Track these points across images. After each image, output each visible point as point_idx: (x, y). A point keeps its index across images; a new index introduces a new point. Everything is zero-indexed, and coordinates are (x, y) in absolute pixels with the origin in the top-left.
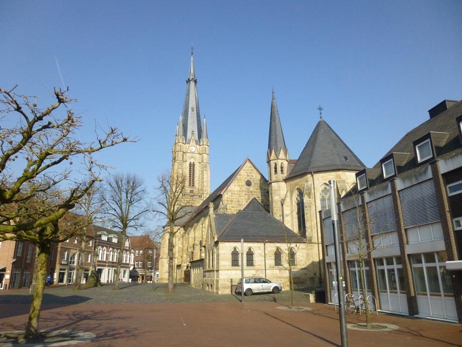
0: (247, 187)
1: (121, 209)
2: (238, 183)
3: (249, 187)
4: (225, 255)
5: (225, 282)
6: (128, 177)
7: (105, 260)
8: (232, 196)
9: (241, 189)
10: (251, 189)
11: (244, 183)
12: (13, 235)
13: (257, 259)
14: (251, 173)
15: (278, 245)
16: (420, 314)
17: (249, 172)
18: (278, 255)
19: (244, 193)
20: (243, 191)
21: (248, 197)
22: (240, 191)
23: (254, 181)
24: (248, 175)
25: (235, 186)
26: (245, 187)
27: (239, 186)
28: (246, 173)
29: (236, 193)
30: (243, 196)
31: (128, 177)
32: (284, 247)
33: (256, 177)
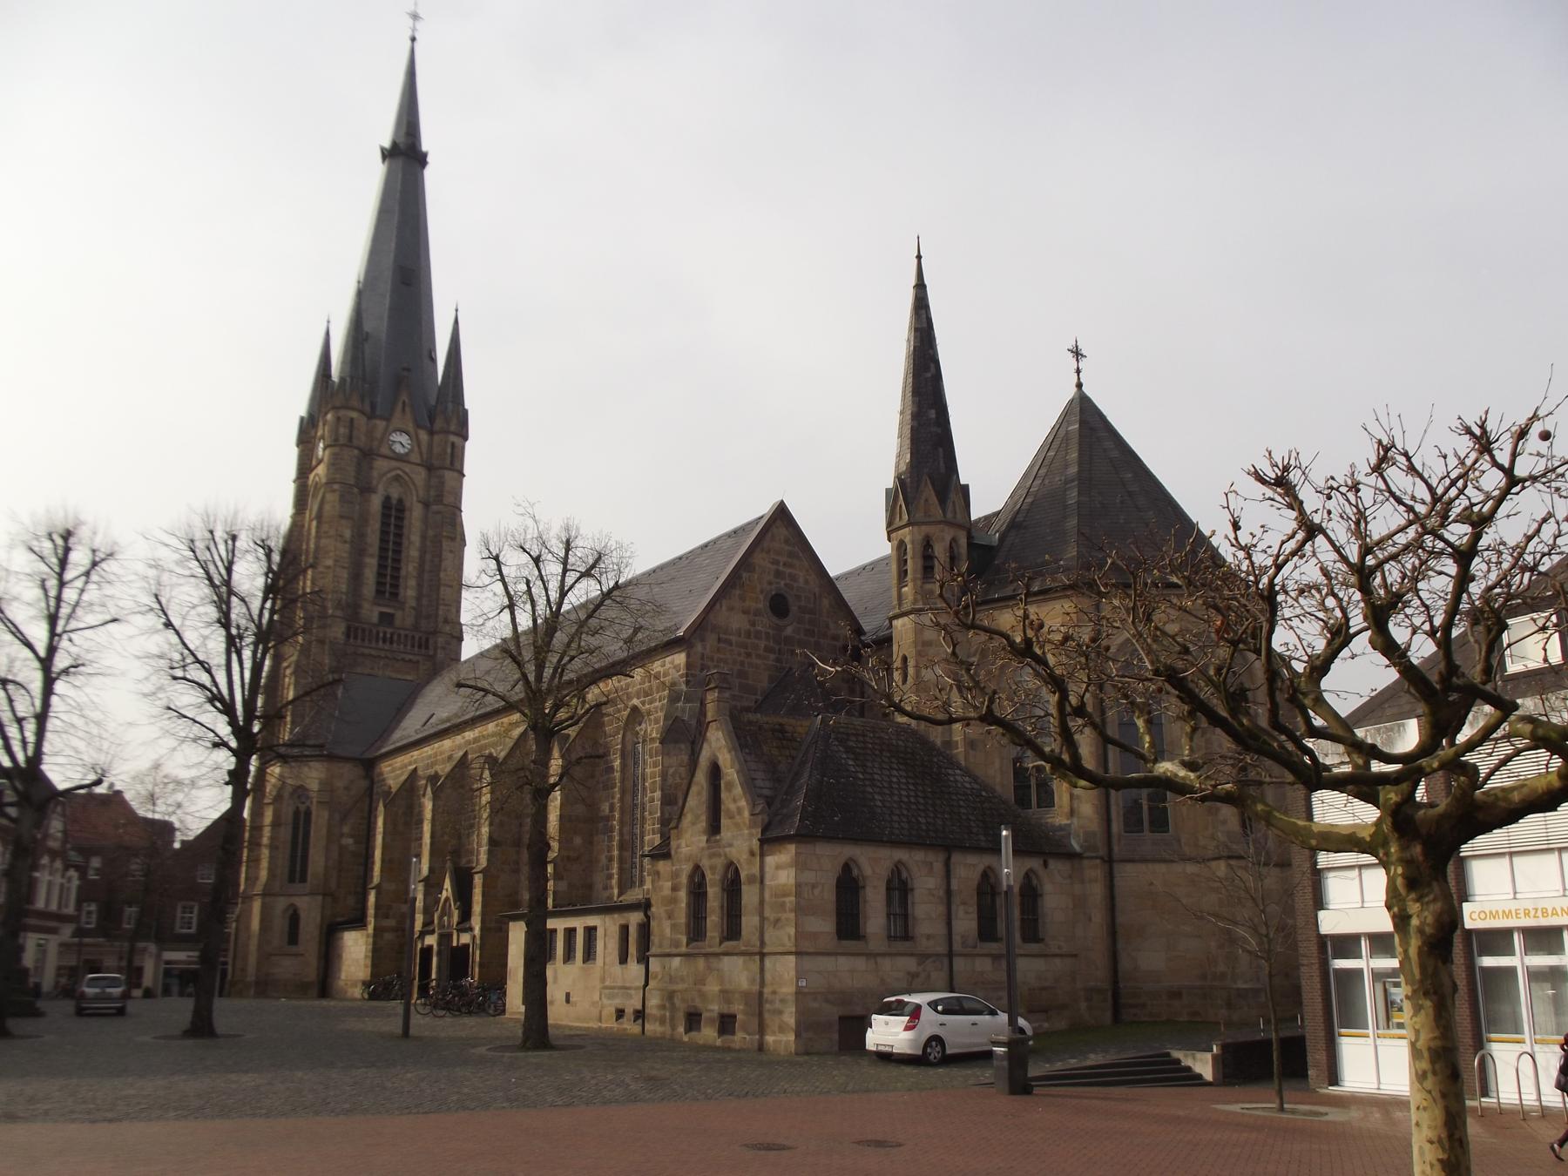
0: (775, 619)
1: (540, 668)
2: (742, 598)
3: (780, 623)
4: (817, 892)
5: (816, 1005)
6: (206, 517)
7: (54, 907)
8: (718, 650)
9: (753, 624)
10: (789, 631)
11: (762, 604)
12: (1366, 814)
13: (926, 911)
14: (791, 566)
15: (901, 854)
16: (1346, 1084)
17: (782, 559)
18: (849, 886)
19: (762, 644)
20: (758, 635)
21: (778, 660)
22: (748, 634)
23: (798, 597)
24: (778, 574)
25: (731, 609)
26: (766, 622)
27: (745, 612)
28: (776, 562)
29: (734, 638)
30: (758, 656)
31: (206, 517)
32: (874, 863)
33: (806, 582)
